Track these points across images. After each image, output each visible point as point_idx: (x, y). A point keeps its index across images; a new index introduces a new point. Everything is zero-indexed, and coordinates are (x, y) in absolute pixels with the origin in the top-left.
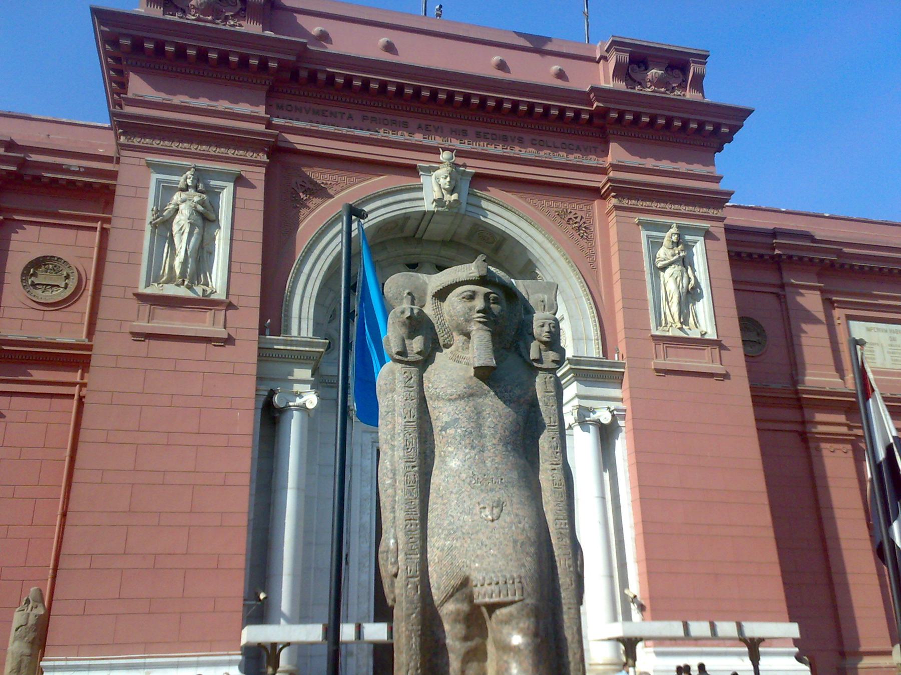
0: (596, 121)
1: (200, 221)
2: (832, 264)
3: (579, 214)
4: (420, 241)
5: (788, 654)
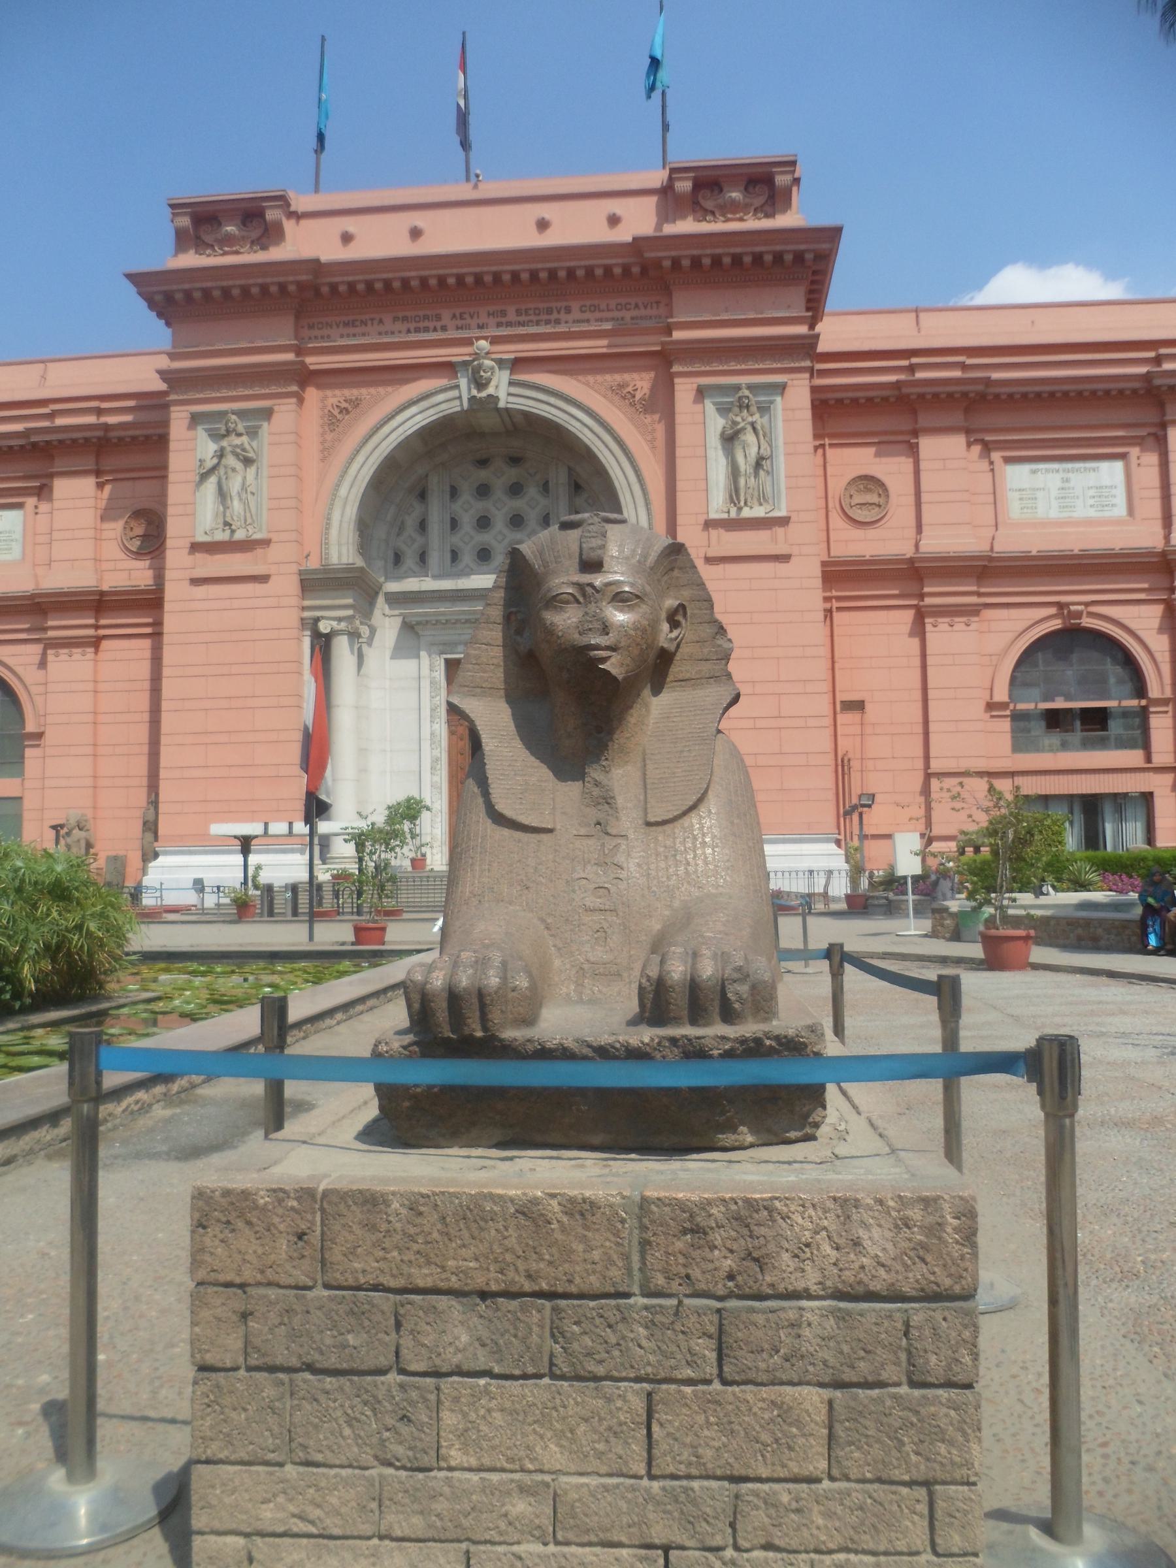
1: (239, 466)
2: (982, 397)
3: (639, 384)
4: (482, 435)
5: (827, 841)
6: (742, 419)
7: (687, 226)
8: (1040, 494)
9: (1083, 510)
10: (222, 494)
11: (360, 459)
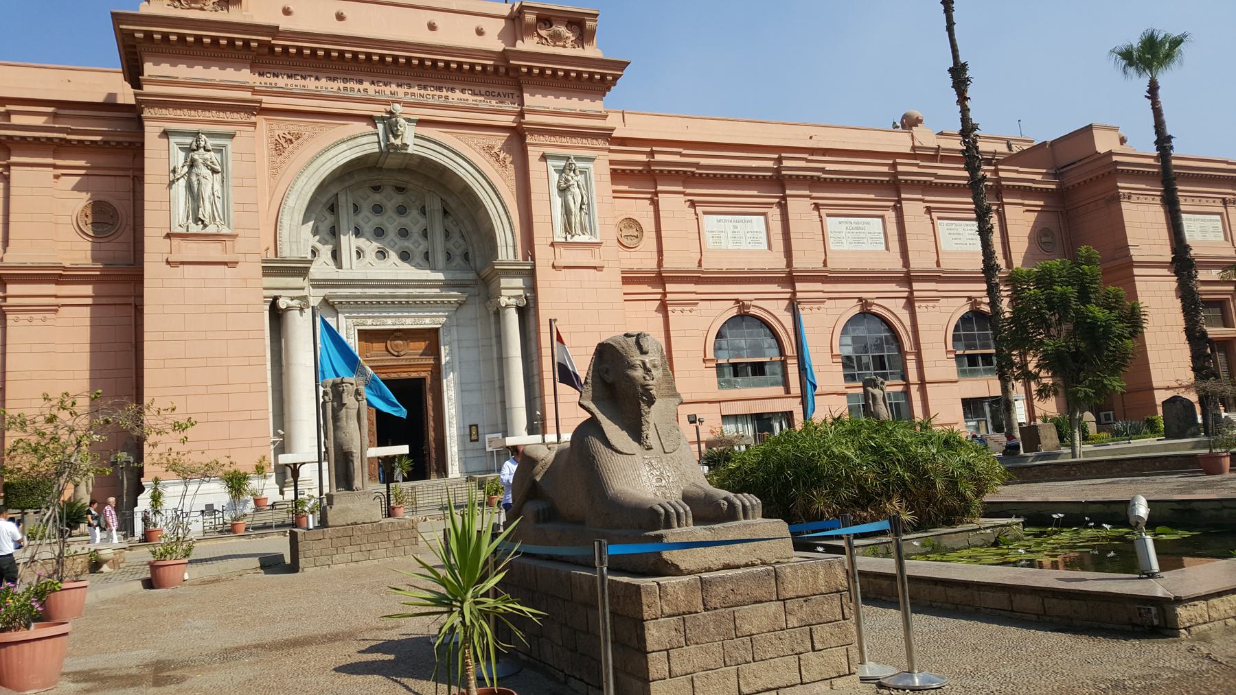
0: (511, 74)
4: (380, 169)
6: (574, 179)
7: (529, 44)
8: (722, 235)
9: (745, 246)
10: (194, 196)
11: (303, 179)
